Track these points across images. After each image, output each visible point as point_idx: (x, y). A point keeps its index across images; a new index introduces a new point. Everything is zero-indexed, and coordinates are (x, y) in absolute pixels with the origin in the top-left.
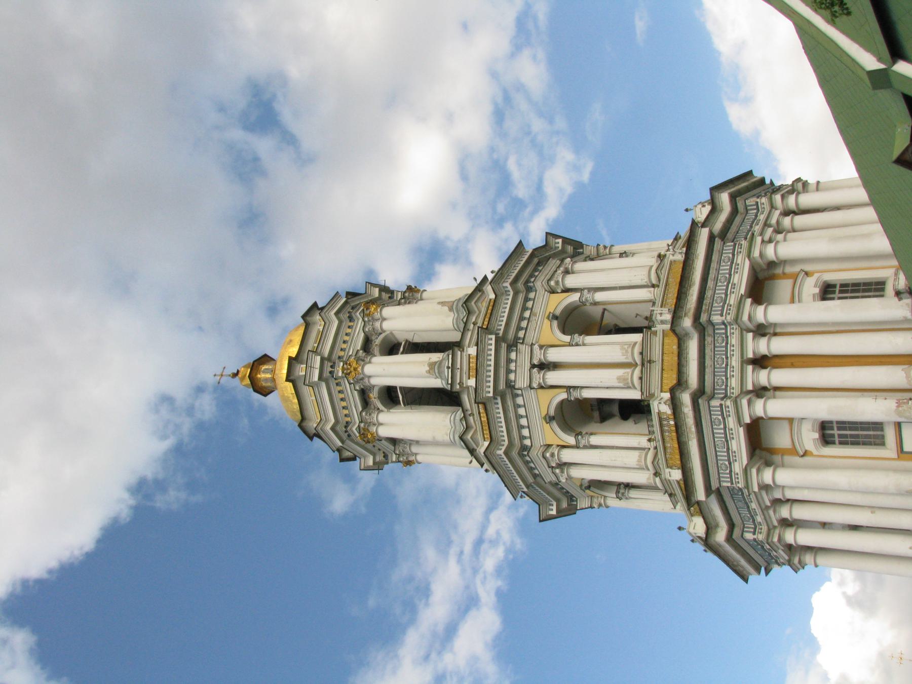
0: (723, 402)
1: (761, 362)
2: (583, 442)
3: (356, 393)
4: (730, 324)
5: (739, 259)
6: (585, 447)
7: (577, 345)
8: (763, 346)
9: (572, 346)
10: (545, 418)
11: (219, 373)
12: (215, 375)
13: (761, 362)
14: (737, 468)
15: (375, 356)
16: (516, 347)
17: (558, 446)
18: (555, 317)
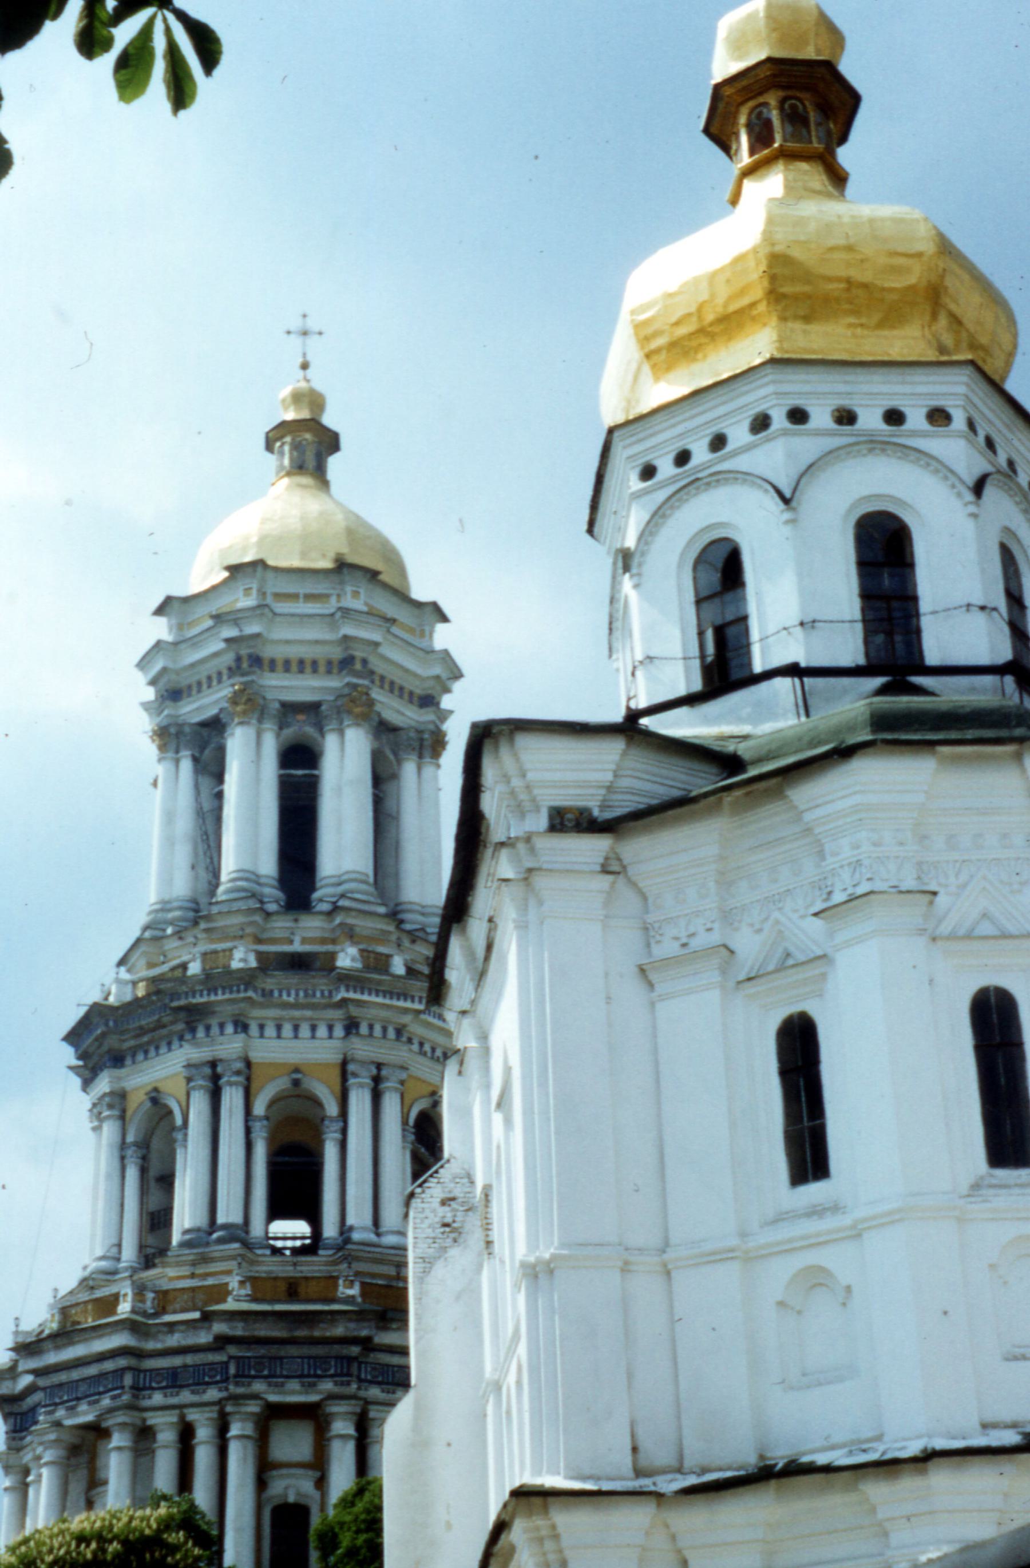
0: (127, 1389)
1: (186, 1434)
2: (129, 1152)
3: (214, 711)
4: (227, 1389)
5: (327, 1386)
6: (123, 1158)
7: (248, 1131)
8: (204, 1433)
9: (247, 1121)
10: (156, 1090)
11: (312, 324)
12: (305, 316)
13: (186, 1434)
14: (60, 1413)
15: (278, 736)
16: (245, 1028)
17: (124, 1111)
18: (296, 1083)
